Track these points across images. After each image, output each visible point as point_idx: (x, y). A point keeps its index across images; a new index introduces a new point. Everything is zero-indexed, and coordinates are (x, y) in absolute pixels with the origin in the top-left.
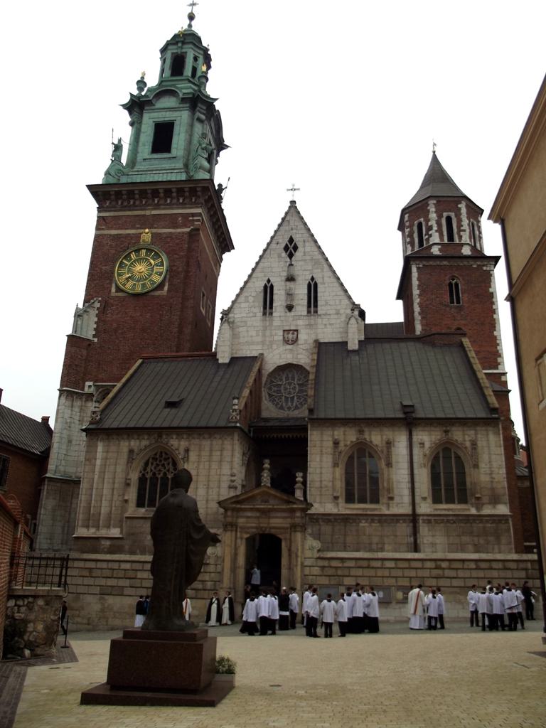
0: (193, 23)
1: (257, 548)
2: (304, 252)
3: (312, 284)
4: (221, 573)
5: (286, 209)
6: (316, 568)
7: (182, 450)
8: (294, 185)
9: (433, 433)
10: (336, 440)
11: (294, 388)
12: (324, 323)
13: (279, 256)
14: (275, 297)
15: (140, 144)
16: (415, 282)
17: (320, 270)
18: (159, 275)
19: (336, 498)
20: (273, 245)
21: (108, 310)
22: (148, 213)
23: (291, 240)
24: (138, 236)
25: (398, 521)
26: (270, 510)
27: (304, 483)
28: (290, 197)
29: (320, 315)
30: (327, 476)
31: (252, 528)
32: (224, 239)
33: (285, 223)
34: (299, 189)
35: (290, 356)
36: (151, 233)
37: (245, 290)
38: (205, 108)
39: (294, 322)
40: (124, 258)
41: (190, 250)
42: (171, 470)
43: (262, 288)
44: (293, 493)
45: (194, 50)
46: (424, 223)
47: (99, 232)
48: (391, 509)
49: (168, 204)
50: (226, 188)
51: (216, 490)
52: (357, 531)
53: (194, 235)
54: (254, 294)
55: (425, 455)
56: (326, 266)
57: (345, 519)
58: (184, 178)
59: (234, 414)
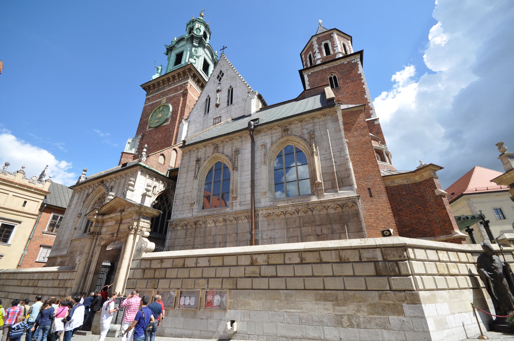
2: (227, 75)
13: (214, 82)
22: (166, 90)
23: (221, 71)
24: (161, 101)
29: (233, 104)
34: (226, 47)
37: (196, 104)
38: (198, 41)
54: (200, 105)
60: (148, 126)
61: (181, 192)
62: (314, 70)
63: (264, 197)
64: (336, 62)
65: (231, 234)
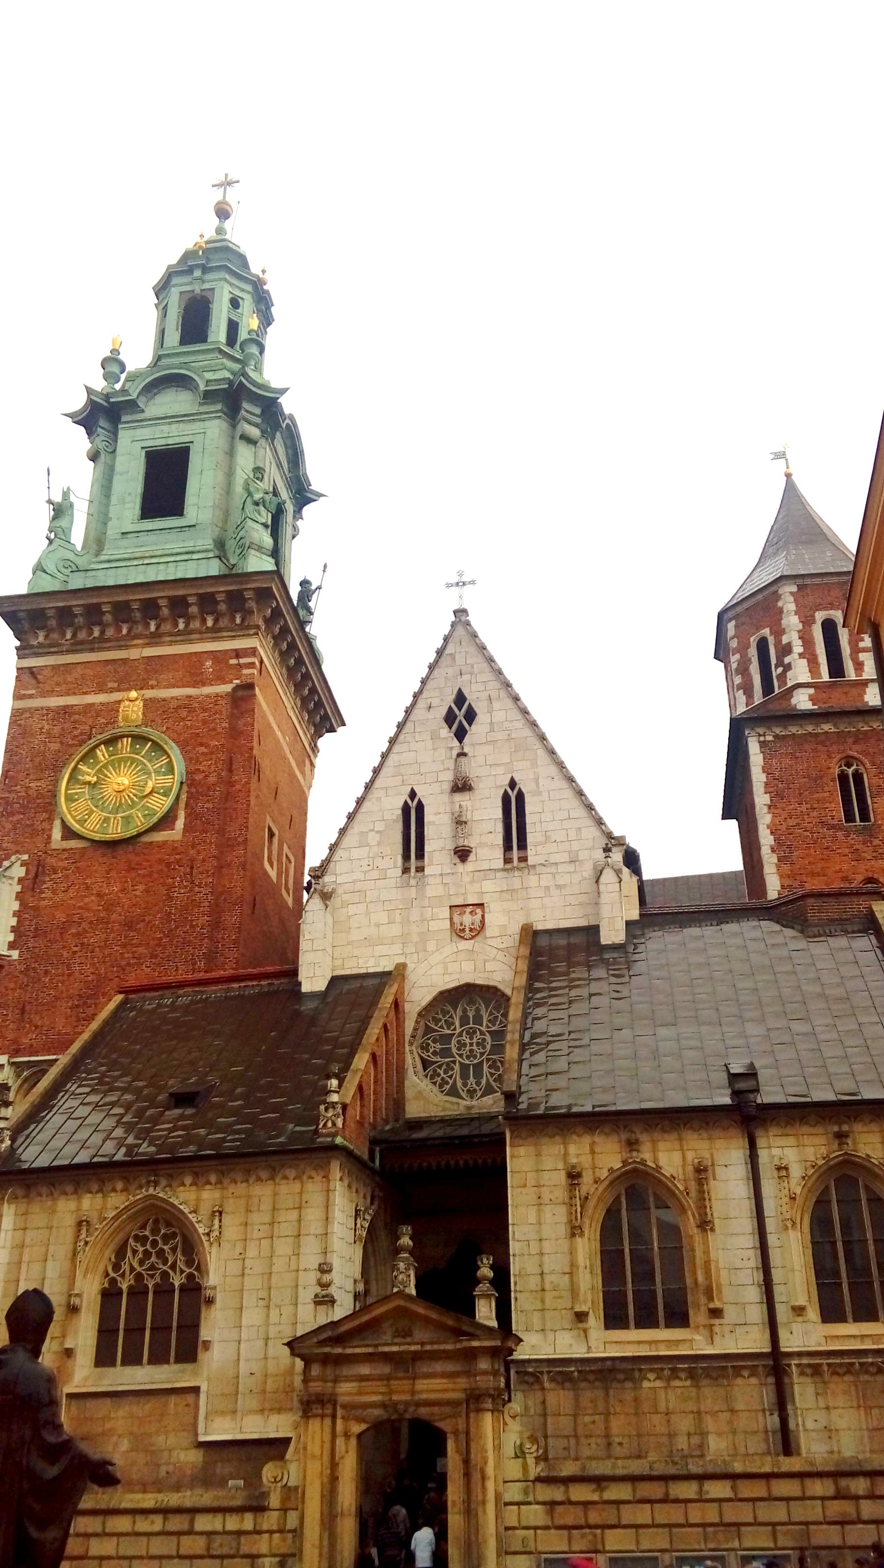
0: (228, 224)
2: (491, 723)
3: (513, 795)
4: (298, 1533)
5: (447, 630)
6: (537, 1507)
7: (205, 1210)
8: (461, 575)
9: (806, 1140)
10: (573, 1167)
11: (480, 1044)
12: (543, 883)
13: (434, 736)
14: (428, 831)
15: (114, 499)
16: (758, 777)
17: (528, 763)
18: (166, 794)
19: (581, 1317)
20: (419, 713)
21: (44, 882)
22: (134, 654)
23: (460, 698)
24: (113, 708)
26: (417, 1357)
29: (534, 866)
30: (556, 1263)
31: (373, 1405)
32: (319, 704)
33: (444, 661)
34: (473, 582)
35: (467, 966)
36: (145, 701)
37: (359, 817)
38: (258, 411)
39: (476, 887)
40: (82, 759)
41: (234, 733)
42: (181, 1264)
43: (400, 812)
44: (470, 1311)
45: (231, 284)
46: (771, 640)
47: (22, 704)
48: (717, 1339)
49: (180, 633)
50: (319, 588)
51: (288, 1310)
54: (380, 826)
56: (541, 753)
58: (214, 572)
59: (330, 1113)
60: (57, 824)
61: (531, 1267)
62: (785, 728)
63: (800, 1319)
64: (867, 718)
65: (717, 1412)
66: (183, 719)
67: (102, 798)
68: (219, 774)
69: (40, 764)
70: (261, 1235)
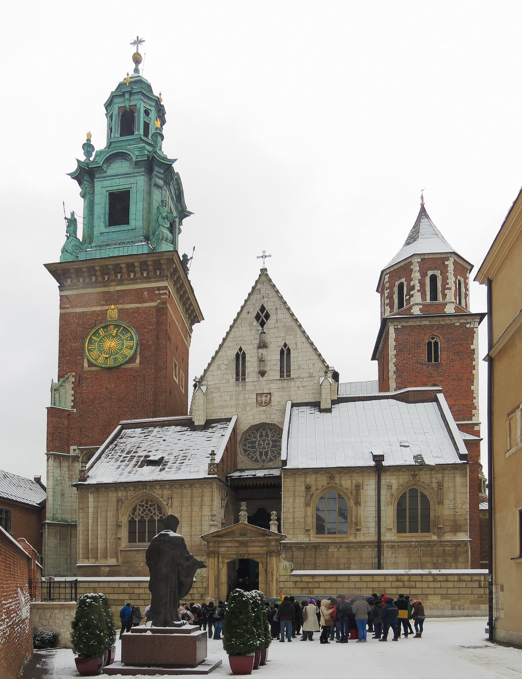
1: (237, 569)
7: (165, 497)
12: (297, 385)
14: (247, 364)
18: (130, 349)
19: (308, 531)
25: (363, 547)
27: (279, 520)
28: (260, 265)
29: (293, 379)
30: (299, 514)
37: (217, 358)
39: (268, 386)
40: (93, 334)
43: (235, 357)
52: (327, 555)
53: (161, 311)
54: (226, 362)
55: (392, 495)
57: (316, 547)
61: (290, 516)
66: (136, 317)
67: (104, 350)
68: (153, 340)
69: (75, 336)
70: (187, 505)
